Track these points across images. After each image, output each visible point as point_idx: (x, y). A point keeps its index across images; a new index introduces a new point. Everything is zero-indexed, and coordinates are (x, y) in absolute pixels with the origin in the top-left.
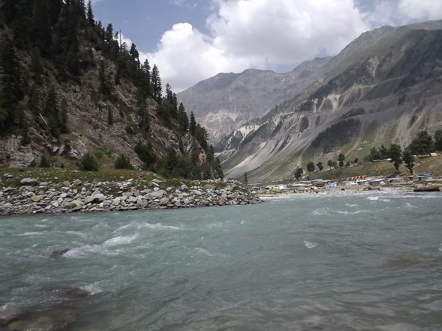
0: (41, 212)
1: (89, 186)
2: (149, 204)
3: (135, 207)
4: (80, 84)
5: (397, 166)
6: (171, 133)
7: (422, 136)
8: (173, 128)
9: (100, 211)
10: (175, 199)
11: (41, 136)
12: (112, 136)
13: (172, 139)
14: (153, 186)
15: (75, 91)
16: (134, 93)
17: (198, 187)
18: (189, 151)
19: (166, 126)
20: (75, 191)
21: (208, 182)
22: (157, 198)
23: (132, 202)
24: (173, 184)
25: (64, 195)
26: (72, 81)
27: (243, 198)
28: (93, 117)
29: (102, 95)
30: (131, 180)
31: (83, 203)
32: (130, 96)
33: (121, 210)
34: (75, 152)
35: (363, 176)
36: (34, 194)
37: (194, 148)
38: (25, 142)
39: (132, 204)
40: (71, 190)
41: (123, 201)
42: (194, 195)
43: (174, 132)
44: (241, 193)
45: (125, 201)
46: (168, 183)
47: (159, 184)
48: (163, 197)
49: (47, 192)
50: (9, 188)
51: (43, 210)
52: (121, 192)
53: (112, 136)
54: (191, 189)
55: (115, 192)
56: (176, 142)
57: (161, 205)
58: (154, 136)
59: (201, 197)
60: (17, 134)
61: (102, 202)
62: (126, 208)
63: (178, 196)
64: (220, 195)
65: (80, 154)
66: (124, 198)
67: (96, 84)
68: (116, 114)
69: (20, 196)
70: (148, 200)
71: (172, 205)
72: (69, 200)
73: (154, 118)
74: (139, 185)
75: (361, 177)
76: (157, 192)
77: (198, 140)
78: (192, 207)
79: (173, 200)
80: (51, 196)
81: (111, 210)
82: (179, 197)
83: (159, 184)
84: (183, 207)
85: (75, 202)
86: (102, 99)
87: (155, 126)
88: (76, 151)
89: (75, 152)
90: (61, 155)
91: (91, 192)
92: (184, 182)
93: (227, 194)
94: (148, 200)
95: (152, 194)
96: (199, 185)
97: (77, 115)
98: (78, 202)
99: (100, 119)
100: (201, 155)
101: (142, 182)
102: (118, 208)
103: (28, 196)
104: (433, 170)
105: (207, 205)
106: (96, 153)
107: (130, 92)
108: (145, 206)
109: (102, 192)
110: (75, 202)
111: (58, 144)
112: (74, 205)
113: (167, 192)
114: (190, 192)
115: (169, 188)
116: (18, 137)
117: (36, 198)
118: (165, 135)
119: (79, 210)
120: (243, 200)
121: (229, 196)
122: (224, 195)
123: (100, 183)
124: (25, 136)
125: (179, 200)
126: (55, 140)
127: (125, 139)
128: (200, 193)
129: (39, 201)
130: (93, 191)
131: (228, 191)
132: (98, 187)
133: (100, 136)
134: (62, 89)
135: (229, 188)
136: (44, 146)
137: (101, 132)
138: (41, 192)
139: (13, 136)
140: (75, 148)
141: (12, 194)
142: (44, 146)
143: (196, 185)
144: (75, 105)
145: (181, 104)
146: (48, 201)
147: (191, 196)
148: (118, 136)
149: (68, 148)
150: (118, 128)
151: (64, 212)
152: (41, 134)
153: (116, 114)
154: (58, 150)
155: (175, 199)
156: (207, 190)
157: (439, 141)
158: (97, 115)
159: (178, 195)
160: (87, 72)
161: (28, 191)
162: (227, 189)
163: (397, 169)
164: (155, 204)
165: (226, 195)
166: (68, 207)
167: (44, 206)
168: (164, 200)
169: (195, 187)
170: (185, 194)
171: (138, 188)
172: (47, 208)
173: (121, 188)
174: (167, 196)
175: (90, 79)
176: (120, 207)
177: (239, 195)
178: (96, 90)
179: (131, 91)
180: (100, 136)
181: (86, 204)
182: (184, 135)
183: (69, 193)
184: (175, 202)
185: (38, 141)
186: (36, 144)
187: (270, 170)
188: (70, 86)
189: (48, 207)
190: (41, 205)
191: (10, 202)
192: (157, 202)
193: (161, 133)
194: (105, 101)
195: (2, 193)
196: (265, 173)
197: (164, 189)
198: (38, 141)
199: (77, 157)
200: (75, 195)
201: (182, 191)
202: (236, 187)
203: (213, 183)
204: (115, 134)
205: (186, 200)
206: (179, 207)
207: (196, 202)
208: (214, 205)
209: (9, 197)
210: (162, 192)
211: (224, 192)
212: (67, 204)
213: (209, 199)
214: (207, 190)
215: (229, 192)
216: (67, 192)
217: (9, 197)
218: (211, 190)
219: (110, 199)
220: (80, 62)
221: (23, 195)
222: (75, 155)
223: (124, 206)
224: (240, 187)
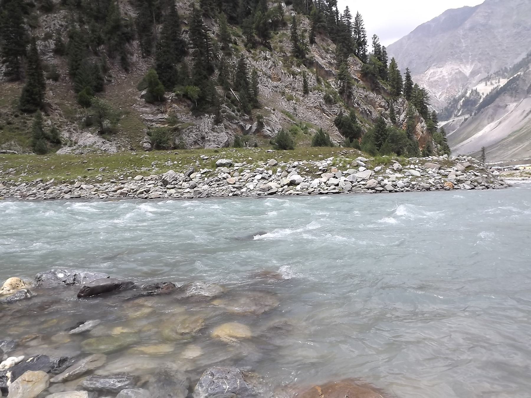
0: (236, 195)
1: (285, 166)
2: (353, 186)
3: (337, 191)
4: (270, 49)
6: (379, 100)
8: (382, 91)
9: (298, 194)
10: (386, 181)
11: (233, 114)
12: (308, 108)
13: (381, 107)
14: (358, 166)
15: (266, 59)
16: (333, 52)
17: (416, 166)
18: (403, 121)
19: (373, 90)
20: (270, 172)
21: (429, 159)
22: (363, 180)
23: (332, 184)
24: (382, 163)
25: (259, 177)
26: (262, 47)
27: (480, 181)
28: (286, 87)
29: (295, 59)
30: (331, 158)
31: (279, 186)
32: (328, 56)
33: (321, 193)
36: (229, 176)
37: (411, 117)
38: (217, 121)
39: (333, 187)
40: (266, 171)
41: (323, 184)
42: (410, 177)
43: (383, 98)
44: (477, 174)
45: (325, 183)
46: (377, 162)
47: (365, 162)
48: (370, 179)
49: (242, 174)
50: (206, 170)
51: (238, 192)
52: (320, 173)
53: (308, 108)
54: (406, 169)
55: (313, 173)
56: (386, 110)
57: (368, 189)
59: (420, 179)
60: (209, 113)
61: (299, 184)
62: (327, 191)
63: (388, 178)
64: (446, 176)
65: (274, 131)
66: (324, 179)
67: (288, 47)
68: (312, 81)
69: (216, 178)
70: (352, 182)
71: (381, 189)
72: (264, 182)
73: (358, 81)
74: (341, 165)
76: (363, 173)
77: (415, 105)
78: (407, 191)
79: (383, 183)
80: (246, 178)
81: (310, 193)
82: (390, 179)
83: (365, 162)
84: (396, 191)
85: (270, 184)
86: (295, 64)
87: (359, 92)
90: (254, 133)
91: (287, 173)
92: (397, 160)
93: (457, 176)
94: (352, 182)
95: (357, 175)
96: (417, 164)
98: (274, 185)
99: (294, 88)
100: (419, 126)
101: (345, 161)
102: (317, 191)
103: (224, 178)
105: (428, 189)
106: (290, 129)
107: (327, 51)
108: (349, 189)
109: (299, 173)
110: (270, 184)
111: (251, 120)
112: (270, 188)
113: (376, 172)
114: (405, 172)
115: (378, 168)
117: (231, 180)
118: (372, 103)
119: (275, 193)
120: (479, 183)
121: (458, 178)
122: (452, 177)
123: (296, 163)
124: (218, 114)
125: (390, 183)
126: (247, 117)
127: (323, 111)
128: (418, 174)
129: (234, 184)
130: (289, 173)
131: (457, 171)
132: (294, 167)
133: (295, 109)
134: (252, 57)
135: (459, 167)
136: (236, 124)
138: (236, 173)
139: (207, 115)
140: (268, 124)
141: (209, 176)
142: (236, 124)
143: (414, 164)
145: (393, 60)
146: (244, 183)
147: (407, 177)
148: (315, 107)
149: (261, 125)
151: (259, 194)
152: (233, 111)
153: (312, 81)
154: (251, 128)
155: (386, 181)
156: (427, 170)
158: (291, 84)
159: (390, 176)
160: (278, 33)
161: (223, 173)
162: (456, 169)
164: (360, 187)
165: (455, 177)
166: (263, 190)
167: (240, 188)
168: (372, 182)
169: (412, 166)
170: (398, 175)
171: (339, 168)
172: (242, 190)
173: (320, 168)
174: (375, 178)
175: (281, 42)
176: (319, 190)
177: (473, 177)
178: (289, 55)
179: (328, 49)
180: (295, 109)
181: (282, 187)
182: (396, 101)
183: (264, 175)
184: (386, 184)
185: (230, 118)
186: (229, 122)
187: (522, 143)
188: (260, 53)
189: (244, 190)
190: (237, 188)
191: (208, 184)
192: (363, 185)
194: (298, 66)
195: (200, 175)
196: (514, 148)
197: (371, 169)
198: (230, 118)
200: (270, 176)
201: (395, 171)
202: (470, 166)
203: (436, 161)
204: (312, 105)
205: (400, 183)
206: (390, 191)
207: (413, 185)
208: (437, 189)
209: (206, 179)
210: (370, 172)
211: (452, 173)
212: (262, 186)
213: (431, 181)
214: (427, 170)
215: (459, 173)
216: (262, 173)
217: (206, 179)
218: (434, 170)
219: (307, 181)
220: (270, 23)
221: (220, 177)
223: (323, 189)
224: (475, 165)
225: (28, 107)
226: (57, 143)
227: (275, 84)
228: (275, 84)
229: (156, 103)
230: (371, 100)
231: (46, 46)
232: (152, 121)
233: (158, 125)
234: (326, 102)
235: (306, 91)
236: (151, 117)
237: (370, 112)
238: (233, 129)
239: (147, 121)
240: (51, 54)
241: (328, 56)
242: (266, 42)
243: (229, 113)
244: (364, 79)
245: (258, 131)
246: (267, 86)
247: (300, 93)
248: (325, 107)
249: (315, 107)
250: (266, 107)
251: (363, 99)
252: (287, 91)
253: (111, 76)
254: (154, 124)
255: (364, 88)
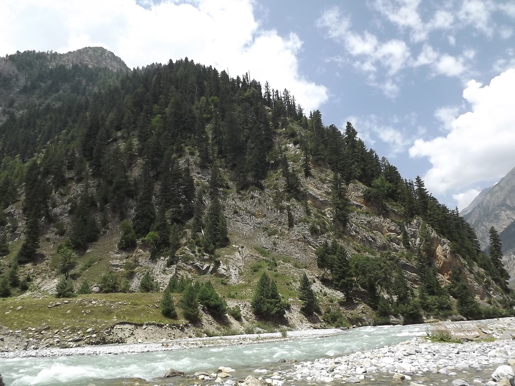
4: (261, 188)
6: (387, 223)
8: (392, 215)
11: (192, 254)
12: (292, 241)
13: (392, 231)
15: (252, 197)
18: (420, 245)
19: (379, 215)
34: (223, 268)
38: (170, 264)
53: (292, 241)
56: (399, 234)
58: (356, 232)
65: (229, 270)
67: (282, 182)
68: (299, 213)
73: (361, 207)
77: (433, 226)
87: (358, 219)
88: (225, 267)
89: (223, 268)
90: (211, 273)
97: (250, 224)
99: (280, 223)
100: (439, 250)
107: (323, 181)
111: (210, 260)
116: (166, 259)
124: (173, 257)
126: (207, 256)
127: (309, 243)
133: (275, 244)
134: (240, 198)
136: (192, 264)
137: (278, 238)
139: (162, 258)
140: (226, 262)
144: (250, 212)
148: (298, 240)
149: (218, 264)
150: (301, 230)
152: (194, 252)
154: (208, 268)
175: (277, 179)
178: (281, 190)
179: (326, 180)
180: (275, 244)
185: (186, 260)
186: (183, 263)
193: (371, 226)
194: (288, 200)
198: (186, 260)
199: (225, 274)
220: (273, 164)
222: (223, 271)
225: (23, 259)
226: (25, 289)
227: (259, 220)
228: (259, 220)
229: (128, 249)
230: (376, 226)
231: (64, 209)
232: (117, 266)
233: (121, 270)
234: (312, 233)
235: (291, 224)
236: (117, 262)
237: (373, 239)
238: (188, 270)
239: (114, 266)
240: (67, 215)
241: (325, 186)
242: (258, 182)
243: (189, 255)
244: (369, 204)
245: (215, 270)
246: (248, 224)
247: (286, 226)
248: (311, 239)
249: (298, 240)
250: (234, 246)
251: (365, 225)
252: (272, 226)
253: (108, 228)
254: (119, 268)
255: (367, 213)
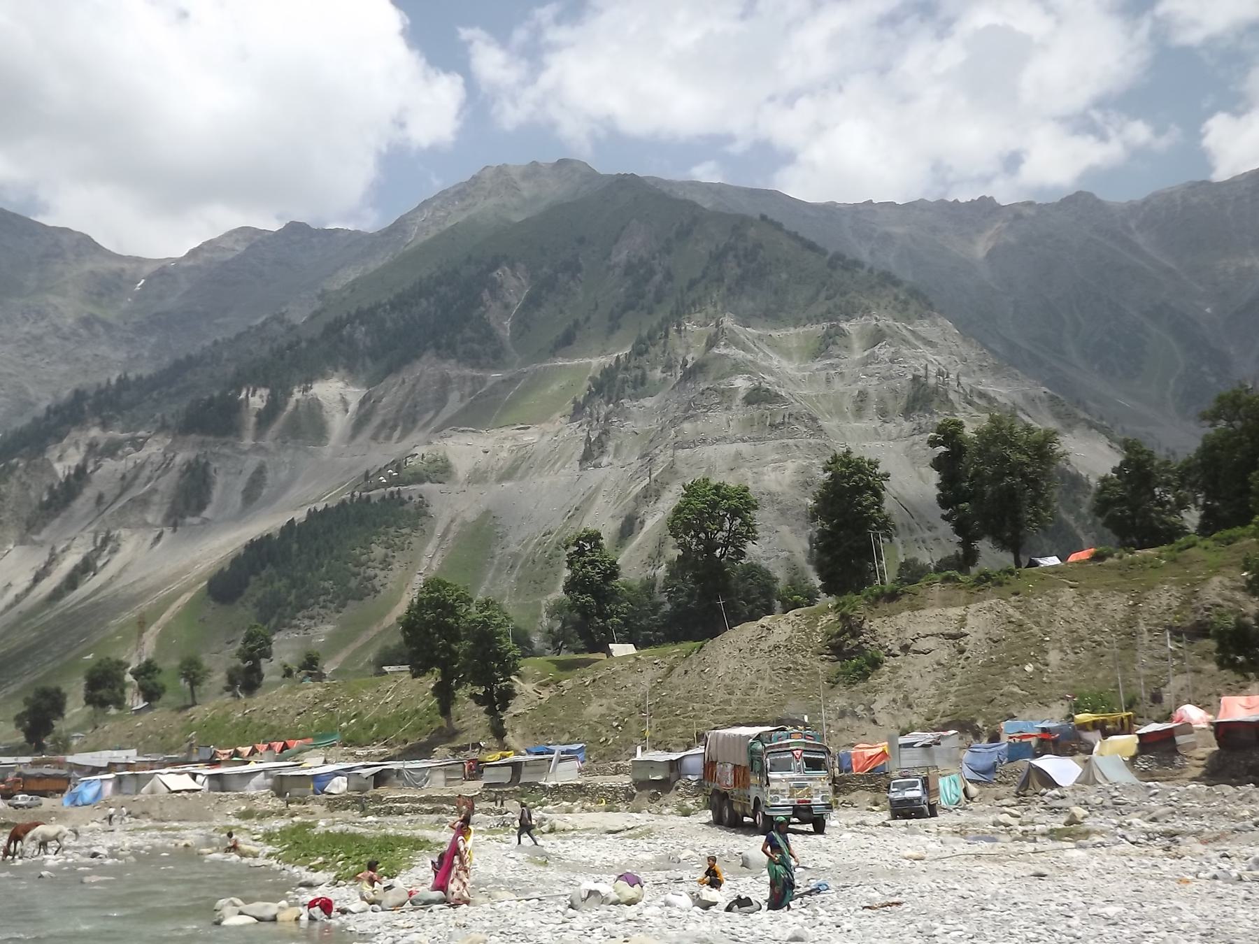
5: (444, 695)
7: (581, 552)
35: (295, 744)
75: (285, 747)
104: (601, 729)
157: (679, 605)
163: (445, 711)
